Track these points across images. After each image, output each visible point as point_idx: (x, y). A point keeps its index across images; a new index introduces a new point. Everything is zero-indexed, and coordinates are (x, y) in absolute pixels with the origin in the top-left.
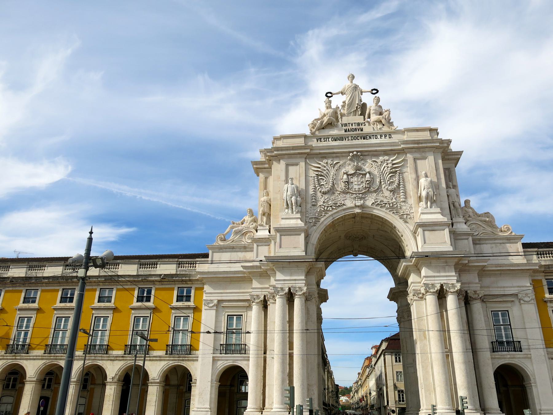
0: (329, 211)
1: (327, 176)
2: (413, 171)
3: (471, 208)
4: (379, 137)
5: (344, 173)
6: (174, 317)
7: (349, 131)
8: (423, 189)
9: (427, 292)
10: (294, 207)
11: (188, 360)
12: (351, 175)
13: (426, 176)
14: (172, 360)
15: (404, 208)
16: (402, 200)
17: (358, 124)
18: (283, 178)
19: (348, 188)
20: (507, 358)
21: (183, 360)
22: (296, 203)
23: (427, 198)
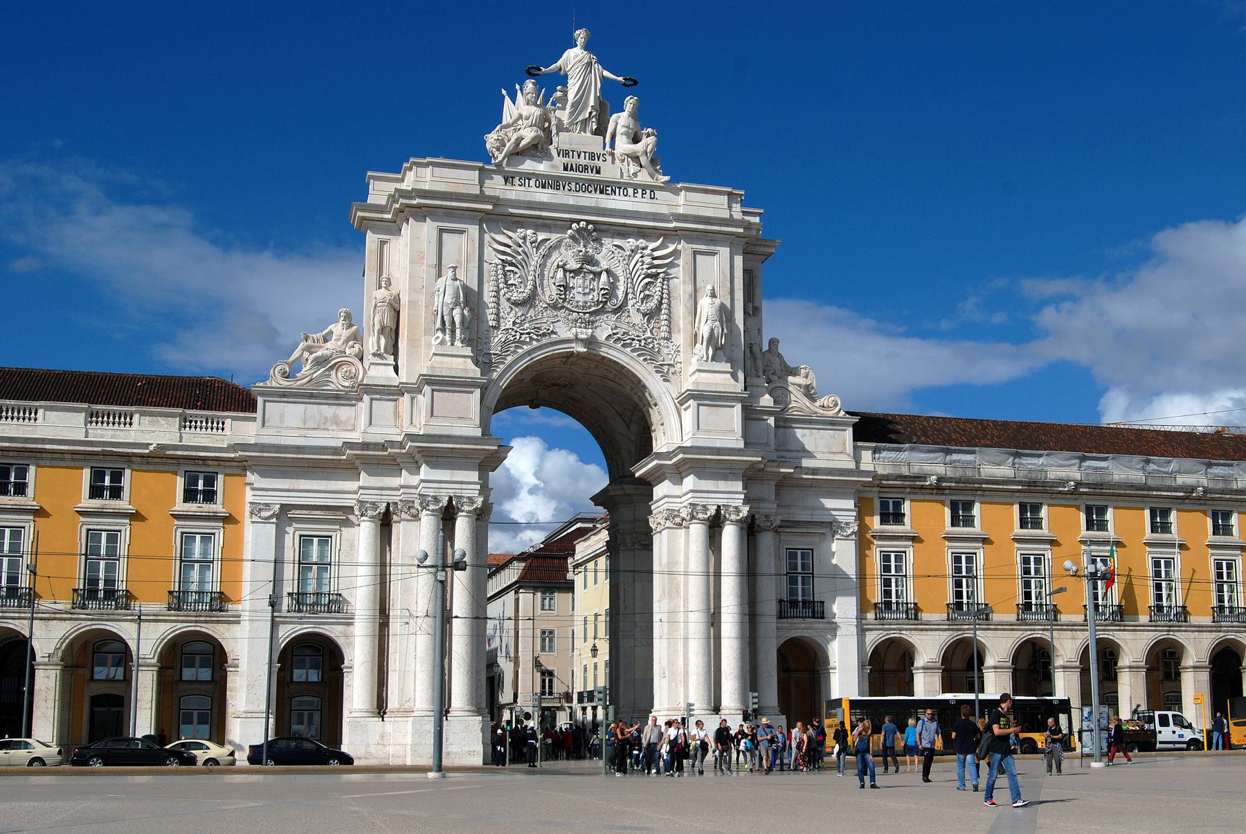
0: (524, 343)
1: (524, 264)
2: (689, 278)
3: (779, 355)
4: (631, 191)
5: (558, 267)
6: (179, 534)
7: (572, 169)
8: (704, 320)
9: (693, 517)
10: (458, 331)
11: (218, 622)
12: (571, 271)
13: (713, 295)
14: (183, 622)
15: (666, 351)
16: (663, 334)
17: (592, 156)
18: (434, 261)
19: (565, 300)
20: (801, 628)
21: (206, 622)
22: (462, 323)
23: (712, 339)
